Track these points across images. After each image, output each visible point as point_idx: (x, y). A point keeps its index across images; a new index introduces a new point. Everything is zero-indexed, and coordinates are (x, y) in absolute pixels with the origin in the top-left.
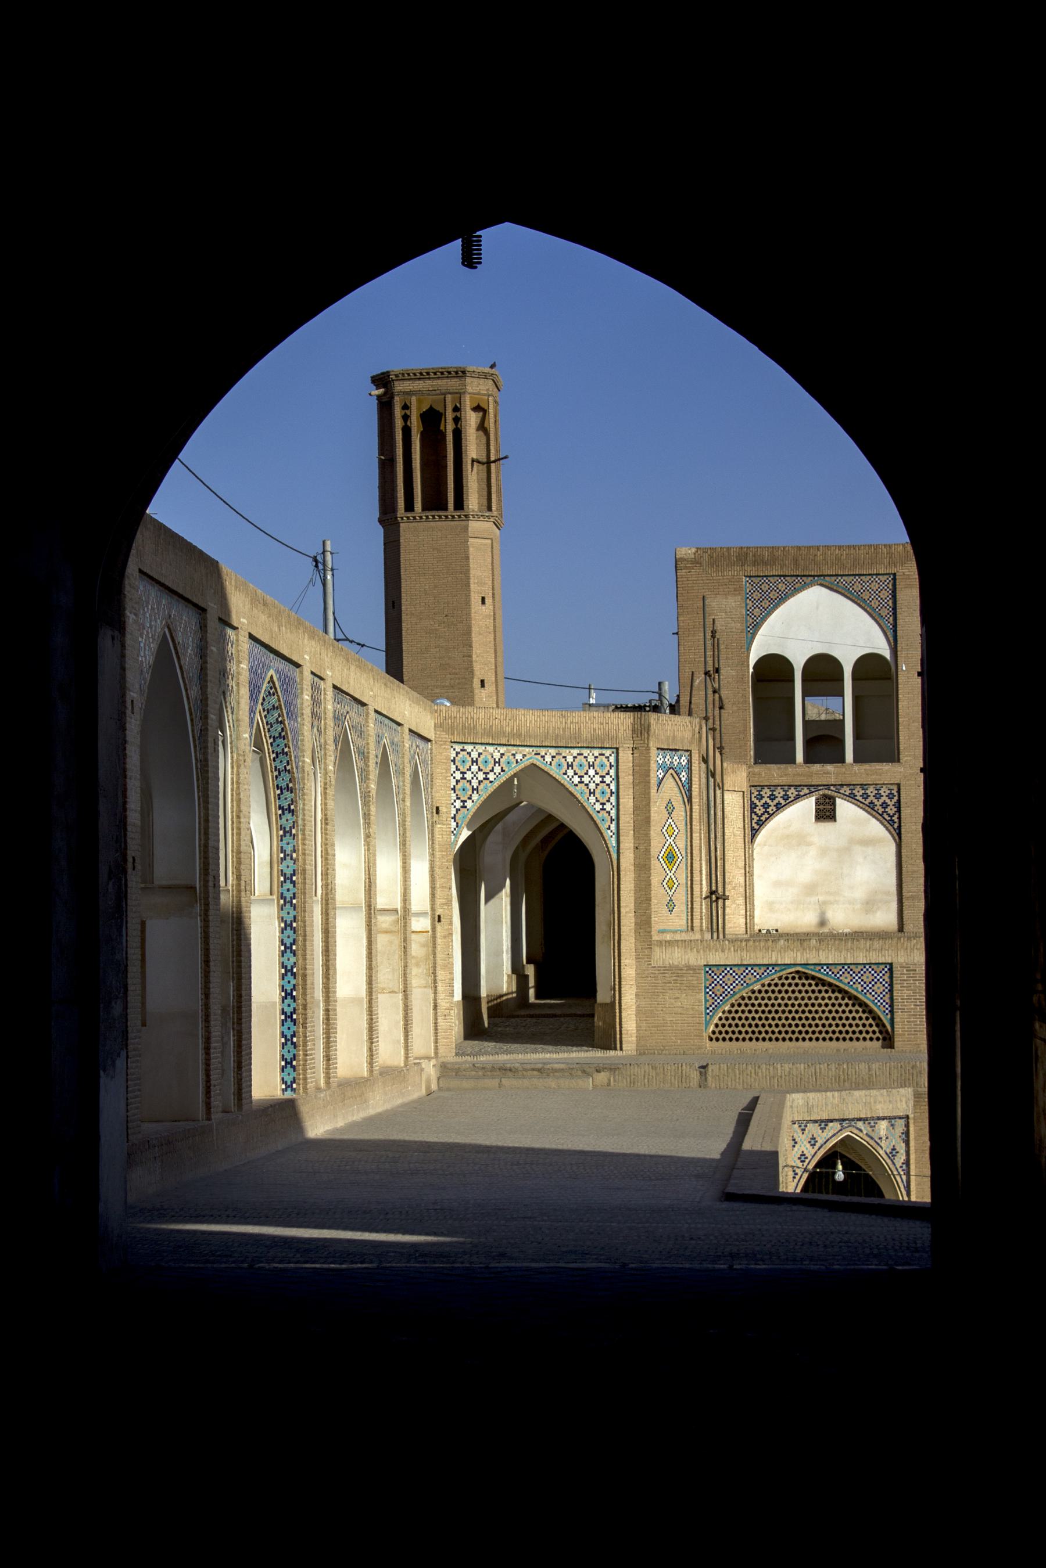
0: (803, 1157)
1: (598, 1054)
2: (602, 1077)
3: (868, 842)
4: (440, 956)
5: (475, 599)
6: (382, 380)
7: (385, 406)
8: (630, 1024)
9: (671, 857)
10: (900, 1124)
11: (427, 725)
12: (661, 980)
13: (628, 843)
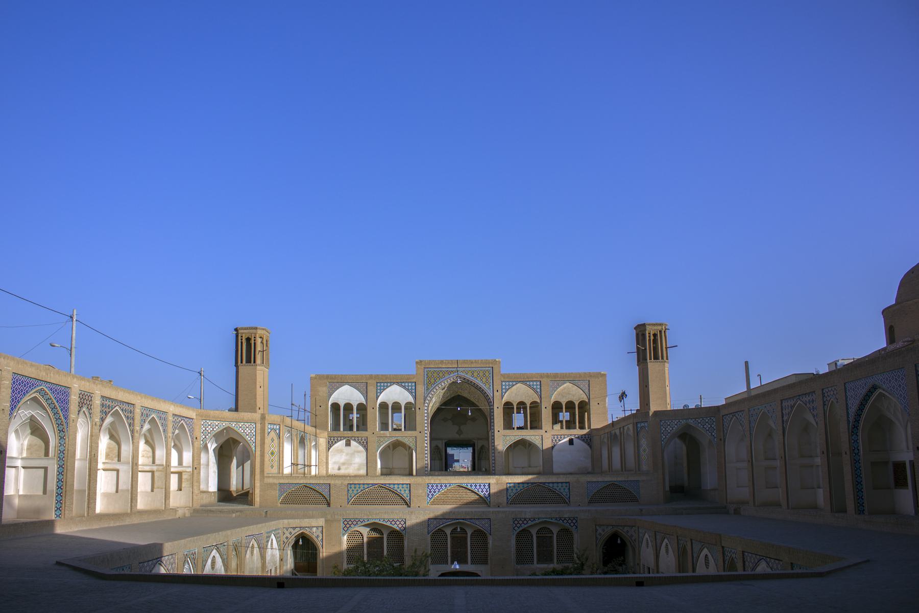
0: (287, 538)
1: (246, 507)
2: (238, 514)
3: (358, 452)
4: (195, 478)
5: (258, 387)
6: (236, 330)
7: (237, 336)
8: (257, 499)
9: (272, 453)
10: (320, 529)
11: (192, 414)
12: (266, 487)
13: (258, 449)
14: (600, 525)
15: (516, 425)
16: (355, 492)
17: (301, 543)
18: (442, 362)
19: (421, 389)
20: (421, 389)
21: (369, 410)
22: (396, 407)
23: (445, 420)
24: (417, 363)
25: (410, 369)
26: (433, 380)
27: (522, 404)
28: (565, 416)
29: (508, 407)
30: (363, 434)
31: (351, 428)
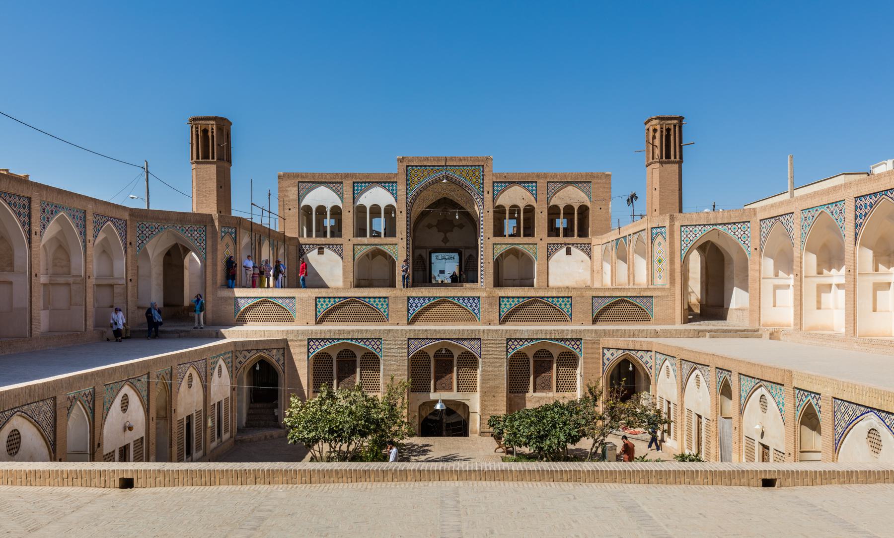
0: (240, 362)
10: (281, 351)
14: (609, 349)
15: (507, 233)
16: (324, 306)
17: (258, 368)
18: (427, 159)
19: (401, 189)
22: (375, 211)
23: (430, 226)
24: (399, 159)
26: (416, 180)
27: (514, 209)
28: (561, 223)
29: (499, 213)
30: (337, 240)
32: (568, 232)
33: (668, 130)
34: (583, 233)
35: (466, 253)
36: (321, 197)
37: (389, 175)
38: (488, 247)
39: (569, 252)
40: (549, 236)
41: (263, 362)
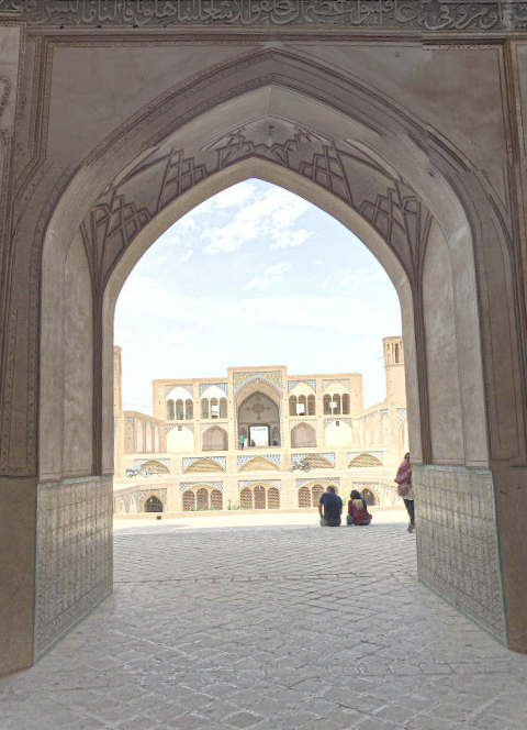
19: (230, 387)
20: (230, 387)
21: (194, 404)
22: (214, 402)
23: (248, 409)
25: (223, 374)
27: (302, 399)
29: (293, 400)
30: (189, 421)
31: (182, 419)
32: (337, 411)
33: (397, 345)
34: (346, 411)
35: (273, 426)
36: (179, 394)
37: (222, 379)
38: (287, 423)
39: (338, 424)
40: (325, 413)
41: (154, 498)
